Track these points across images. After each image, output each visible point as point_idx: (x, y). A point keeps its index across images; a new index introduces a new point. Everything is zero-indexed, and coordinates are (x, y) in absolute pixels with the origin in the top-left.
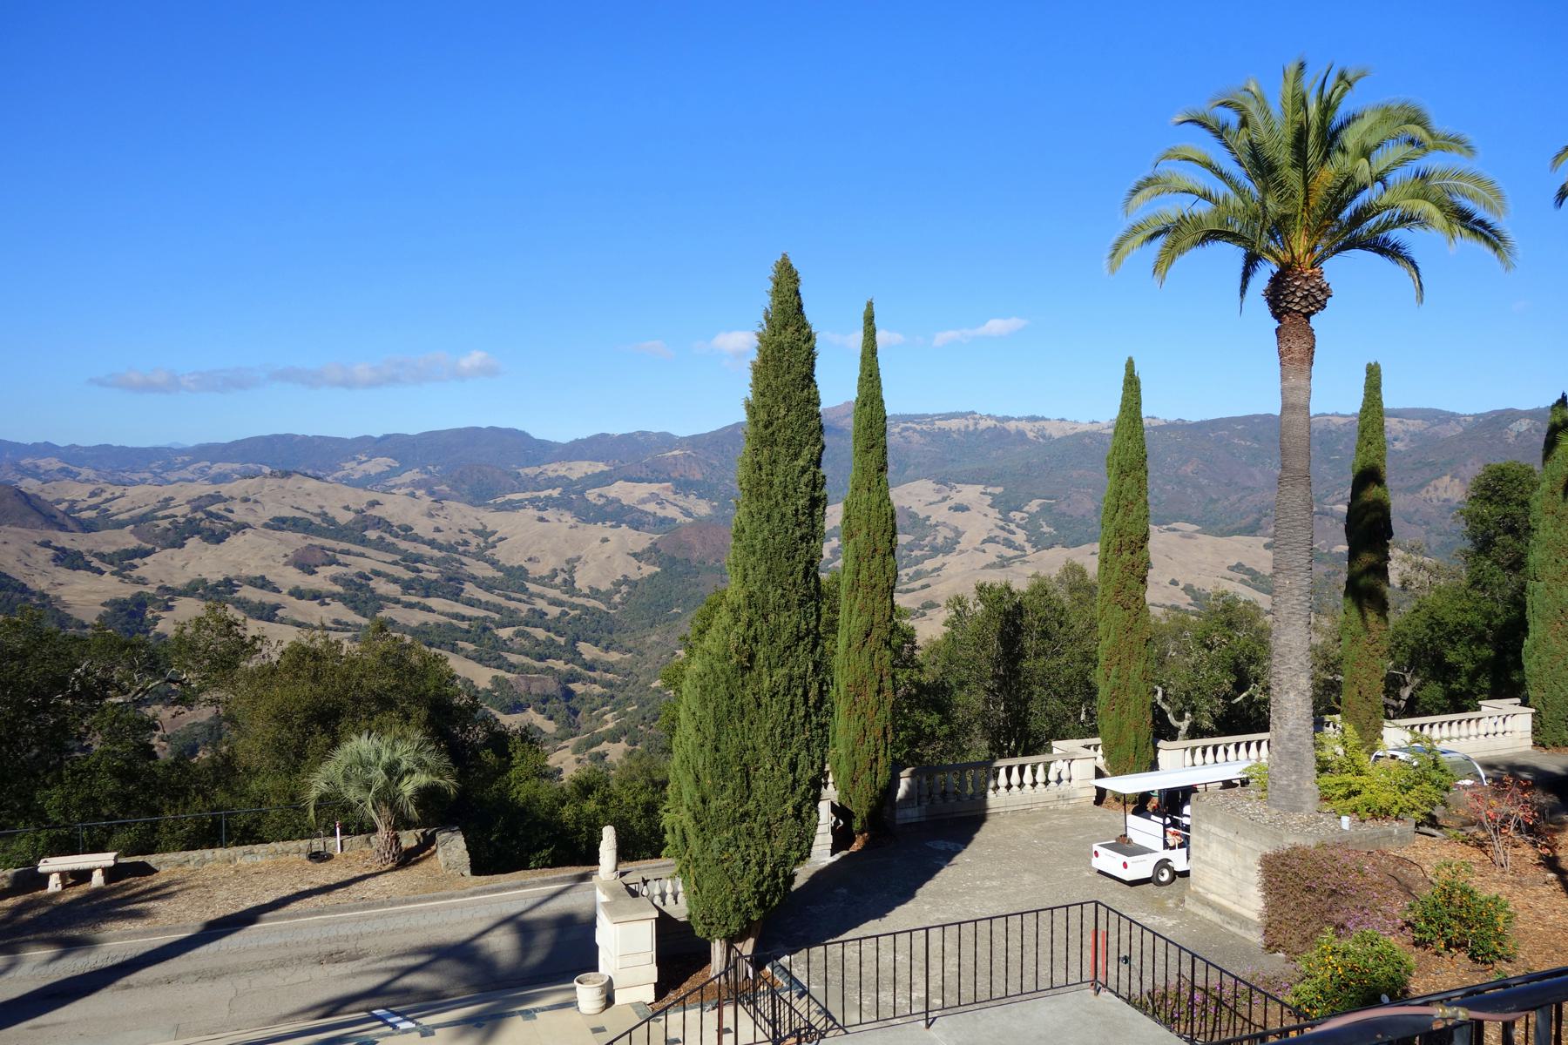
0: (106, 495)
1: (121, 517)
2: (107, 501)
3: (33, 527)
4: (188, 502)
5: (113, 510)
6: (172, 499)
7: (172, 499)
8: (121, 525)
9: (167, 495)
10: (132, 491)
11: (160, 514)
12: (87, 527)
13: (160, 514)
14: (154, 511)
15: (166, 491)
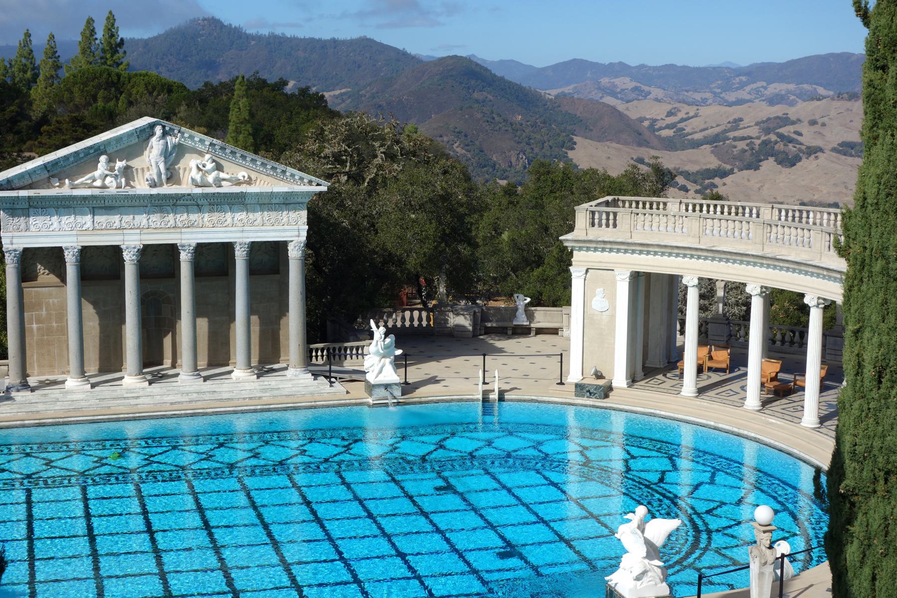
0: (681, 115)
1: (696, 136)
2: (683, 120)
3: (626, 143)
4: (757, 124)
5: (688, 130)
6: (741, 120)
7: (741, 120)
8: (696, 145)
9: (736, 116)
10: (704, 111)
11: (731, 135)
12: (670, 145)
13: (731, 135)
14: (725, 131)
15: (736, 112)
